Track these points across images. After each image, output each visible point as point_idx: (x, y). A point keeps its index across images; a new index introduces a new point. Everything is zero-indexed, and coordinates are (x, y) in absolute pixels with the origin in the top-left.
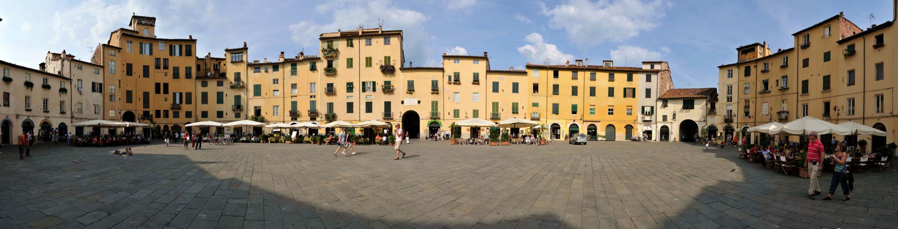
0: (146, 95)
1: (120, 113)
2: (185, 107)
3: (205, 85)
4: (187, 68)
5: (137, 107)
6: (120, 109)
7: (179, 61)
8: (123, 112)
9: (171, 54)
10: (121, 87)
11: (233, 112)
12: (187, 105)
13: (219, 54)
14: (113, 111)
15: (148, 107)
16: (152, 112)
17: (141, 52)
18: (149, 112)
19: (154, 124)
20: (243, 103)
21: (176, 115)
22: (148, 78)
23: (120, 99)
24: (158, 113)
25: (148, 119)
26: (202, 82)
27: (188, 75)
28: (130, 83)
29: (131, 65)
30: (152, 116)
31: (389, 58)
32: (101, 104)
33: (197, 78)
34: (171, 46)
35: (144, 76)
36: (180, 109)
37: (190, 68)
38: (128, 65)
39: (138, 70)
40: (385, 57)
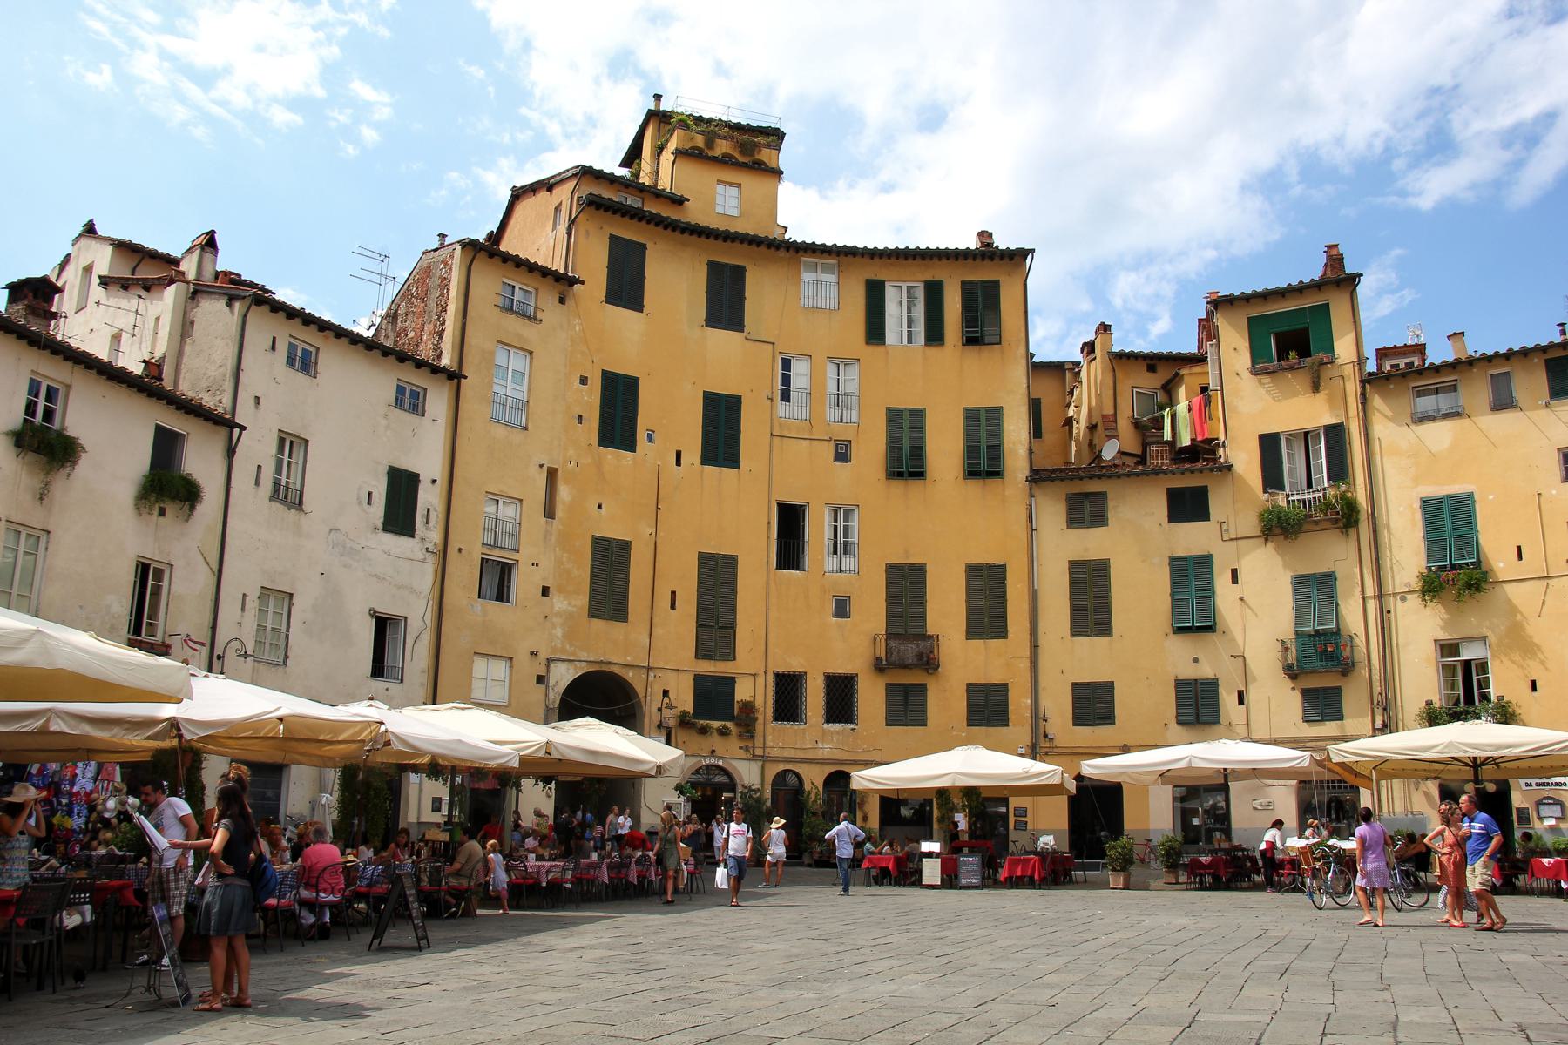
4: (971, 416)
6: (543, 656)
8: (563, 676)
10: (560, 512)
11: (1289, 683)
14: (500, 669)
15: (729, 654)
16: (753, 690)
18: (730, 682)
19: (765, 759)
23: (545, 591)
24: (788, 692)
25: (723, 732)
29: (631, 384)
30: (748, 707)
33: (1038, 477)
37: (994, 416)
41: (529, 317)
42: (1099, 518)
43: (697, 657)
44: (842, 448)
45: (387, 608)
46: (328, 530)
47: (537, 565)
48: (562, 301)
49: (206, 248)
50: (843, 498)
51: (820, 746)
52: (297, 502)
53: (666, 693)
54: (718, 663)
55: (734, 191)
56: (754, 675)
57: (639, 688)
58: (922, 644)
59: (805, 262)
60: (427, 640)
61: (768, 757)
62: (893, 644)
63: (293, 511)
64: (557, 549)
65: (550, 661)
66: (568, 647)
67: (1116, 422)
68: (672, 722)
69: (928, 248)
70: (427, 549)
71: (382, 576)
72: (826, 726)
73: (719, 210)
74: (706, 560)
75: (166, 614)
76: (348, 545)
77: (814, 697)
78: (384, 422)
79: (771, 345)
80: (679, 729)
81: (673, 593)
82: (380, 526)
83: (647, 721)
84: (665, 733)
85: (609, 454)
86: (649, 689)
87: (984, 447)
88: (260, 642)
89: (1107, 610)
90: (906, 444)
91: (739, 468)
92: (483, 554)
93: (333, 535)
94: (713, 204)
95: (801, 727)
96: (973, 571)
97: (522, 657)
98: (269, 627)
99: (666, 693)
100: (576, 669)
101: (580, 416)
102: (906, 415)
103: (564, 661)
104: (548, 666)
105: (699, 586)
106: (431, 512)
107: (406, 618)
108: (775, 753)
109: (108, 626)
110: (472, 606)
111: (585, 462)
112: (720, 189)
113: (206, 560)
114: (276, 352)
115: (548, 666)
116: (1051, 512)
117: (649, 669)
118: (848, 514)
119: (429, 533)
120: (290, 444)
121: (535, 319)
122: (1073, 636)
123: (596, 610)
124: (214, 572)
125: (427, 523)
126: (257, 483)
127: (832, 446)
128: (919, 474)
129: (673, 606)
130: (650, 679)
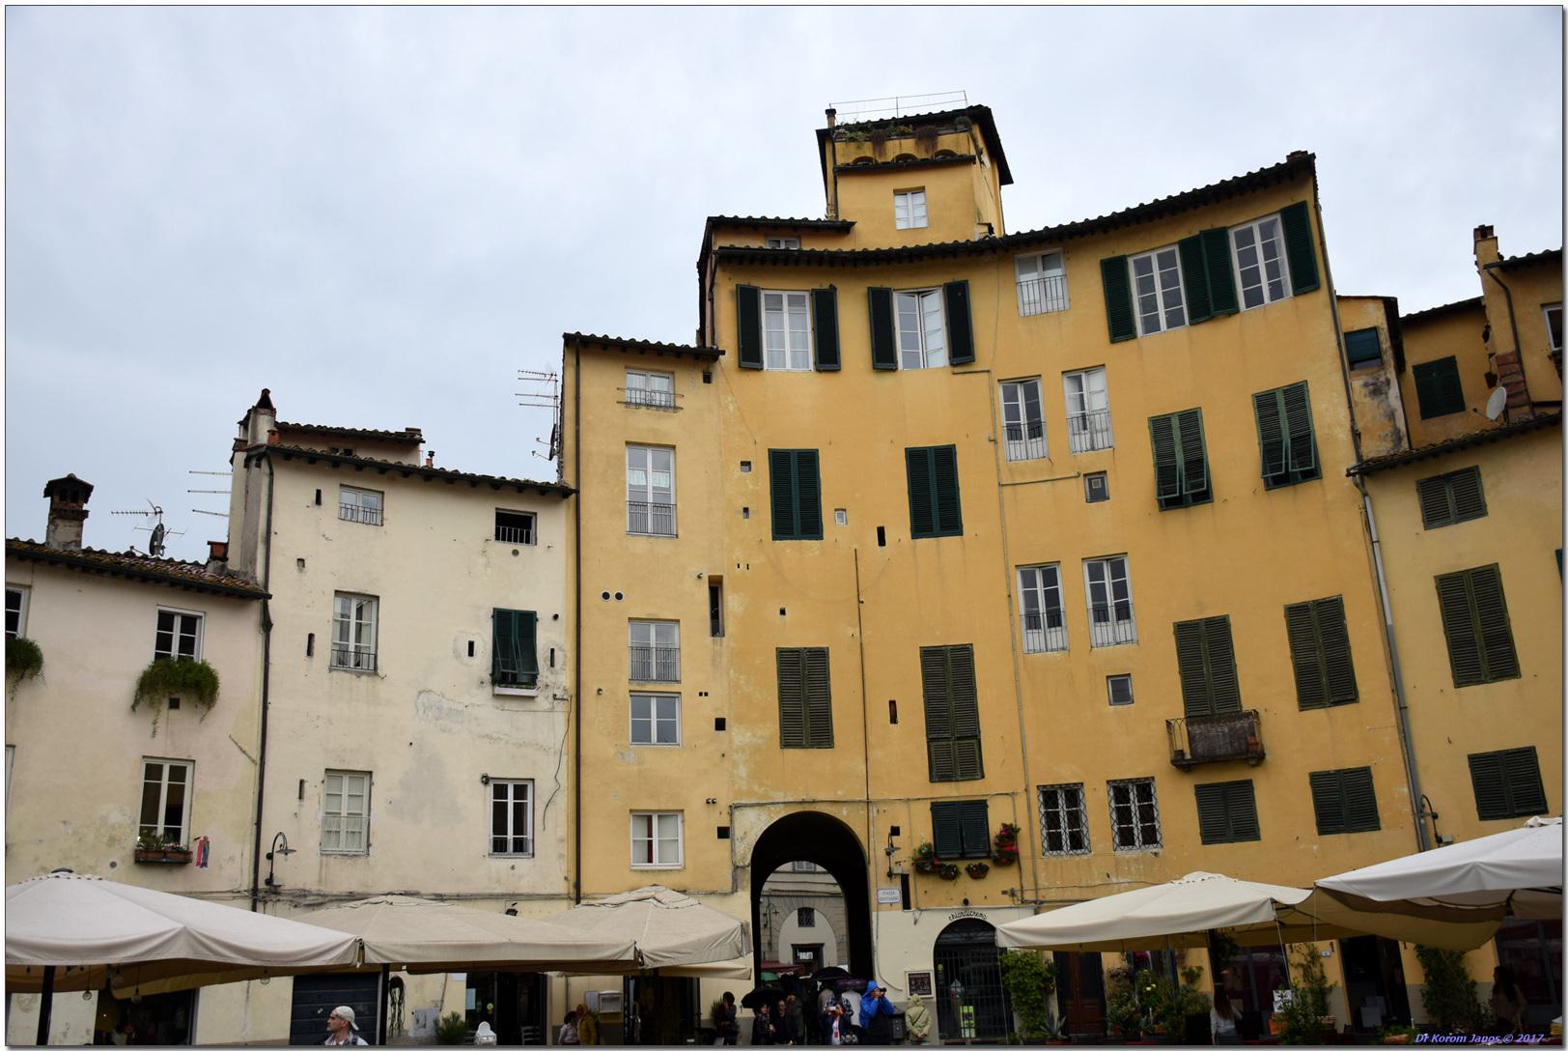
1: (724, 833)
4: (1265, 403)
6: (724, 803)
8: (752, 826)
9: (1121, 327)
10: (730, 623)
12: (1317, 715)
15: (973, 768)
17: (883, 356)
18: (980, 807)
22: (949, 542)
23: (720, 724)
29: (808, 461)
32: (549, 778)
33: (1368, 472)
34: (1114, 275)
37: (1297, 395)
38: (780, 461)
41: (666, 408)
42: (1472, 506)
43: (932, 780)
44: (1096, 483)
45: (509, 770)
46: (415, 693)
47: (701, 694)
48: (707, 379)
49: (259, 410)
50: (1105, 546)
51: (1114, 880)
52: (372, 667)
53: (895, 831)
54: (961, 784)
55: (920, 198)
56: (1012, 795)
57: (859, 831)
58: (1238, 724)
59: (1019, 260)
60: (564, 802)
61: (1042, 903)
62: (1197, 730)
63: (364, 678)
64: (732, 671)
65: (734, 808)
66: (756, 788)
67: (1520, 361)
68: (906, 867)
69: (1170, 197)
70: (555, 695)
71: (494, 735)
72: (1119, 853)
73: (901, 225)
74: (932, 658)
75: (190, 815)
76: (445, 706)
78: (482, 560)
79: (985, 375)
80: (919, 878)
81: (892, 703)
82: (487, 678)
83: (872, 870)
84: (898, 882)
85: (788, 546)
86: (871, 828)
87: (1287, 440)
88: (353, 833)
89: (1506, 639)
90: (1180, 460)
91: (961, 534)
92: (630, 691)
93: (423, 698)
94: (892, 220)
95: (1085, 857)
96: (1298, 616)
97: (695, 806)
98: (344, 813)
99: (895, 831)
100: (769, 815)
101: (746, 510)
102: (1175, 423)
103: (752, 806)
104: (731, 815)
105: (926, 690)
106: (557, 653)
107: (533, 780)
108: (1052, 895)
109: (105, 840)
110: (622, 754)
111: (757, 562)
112: (900, 201)
113: (241, 749)
114: (322, 507)
115: (731, 815)
117: (868, 802)
118: (1118, 569)
119: (555, 678)
120: (362, 603)
121: (676, 408)
122: (1458, 685)
123: (790, 738)
124: (253, 761)
125: (552, 665)
126: (310, 652)
127: (1082, 477)
128: (1204, 496)
129: (894, 720)
130: (871, 815)
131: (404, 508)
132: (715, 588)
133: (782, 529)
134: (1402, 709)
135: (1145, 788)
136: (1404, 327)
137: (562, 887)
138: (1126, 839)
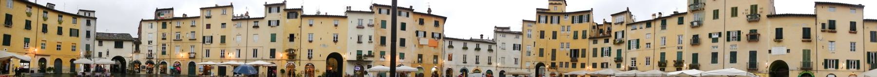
0: (554, 51)
2: (581, 60)
3: (595, 42)
4: (583, 31)
5: (547, 60)
7: (580, 27)
8: (536, 63)
9: (573, 22)
13: (609, 20)
15: (555, 60)
17: (552, 22)
18: (555, 63)
20: (623, 55)
21: (574, 66)
22: (555, 40)
24: (561, 63)
26: (594, 41)
27: (584, 37)
28: (542, 44)
29: (544, 31)
31: (756, 6)
34: (573, 18)
35: (553, 38)
36: (577, 61)
37: (586, 31)
38: (541, 31)
39: (549, 35)
40: (752, 6)
42: (597, 43)
45: (516, 58)
50: (568, 42)
77: (564, 64)
85: (541, 39)
116: (592, 42)
128: (577, 39)
131: (508, 36)
132: (535, 43)
133: (541, 38)
134: (588, 59)
135: (568, 63)
136: (598, 25)
137: (520, 67)
138: (566, 67)
